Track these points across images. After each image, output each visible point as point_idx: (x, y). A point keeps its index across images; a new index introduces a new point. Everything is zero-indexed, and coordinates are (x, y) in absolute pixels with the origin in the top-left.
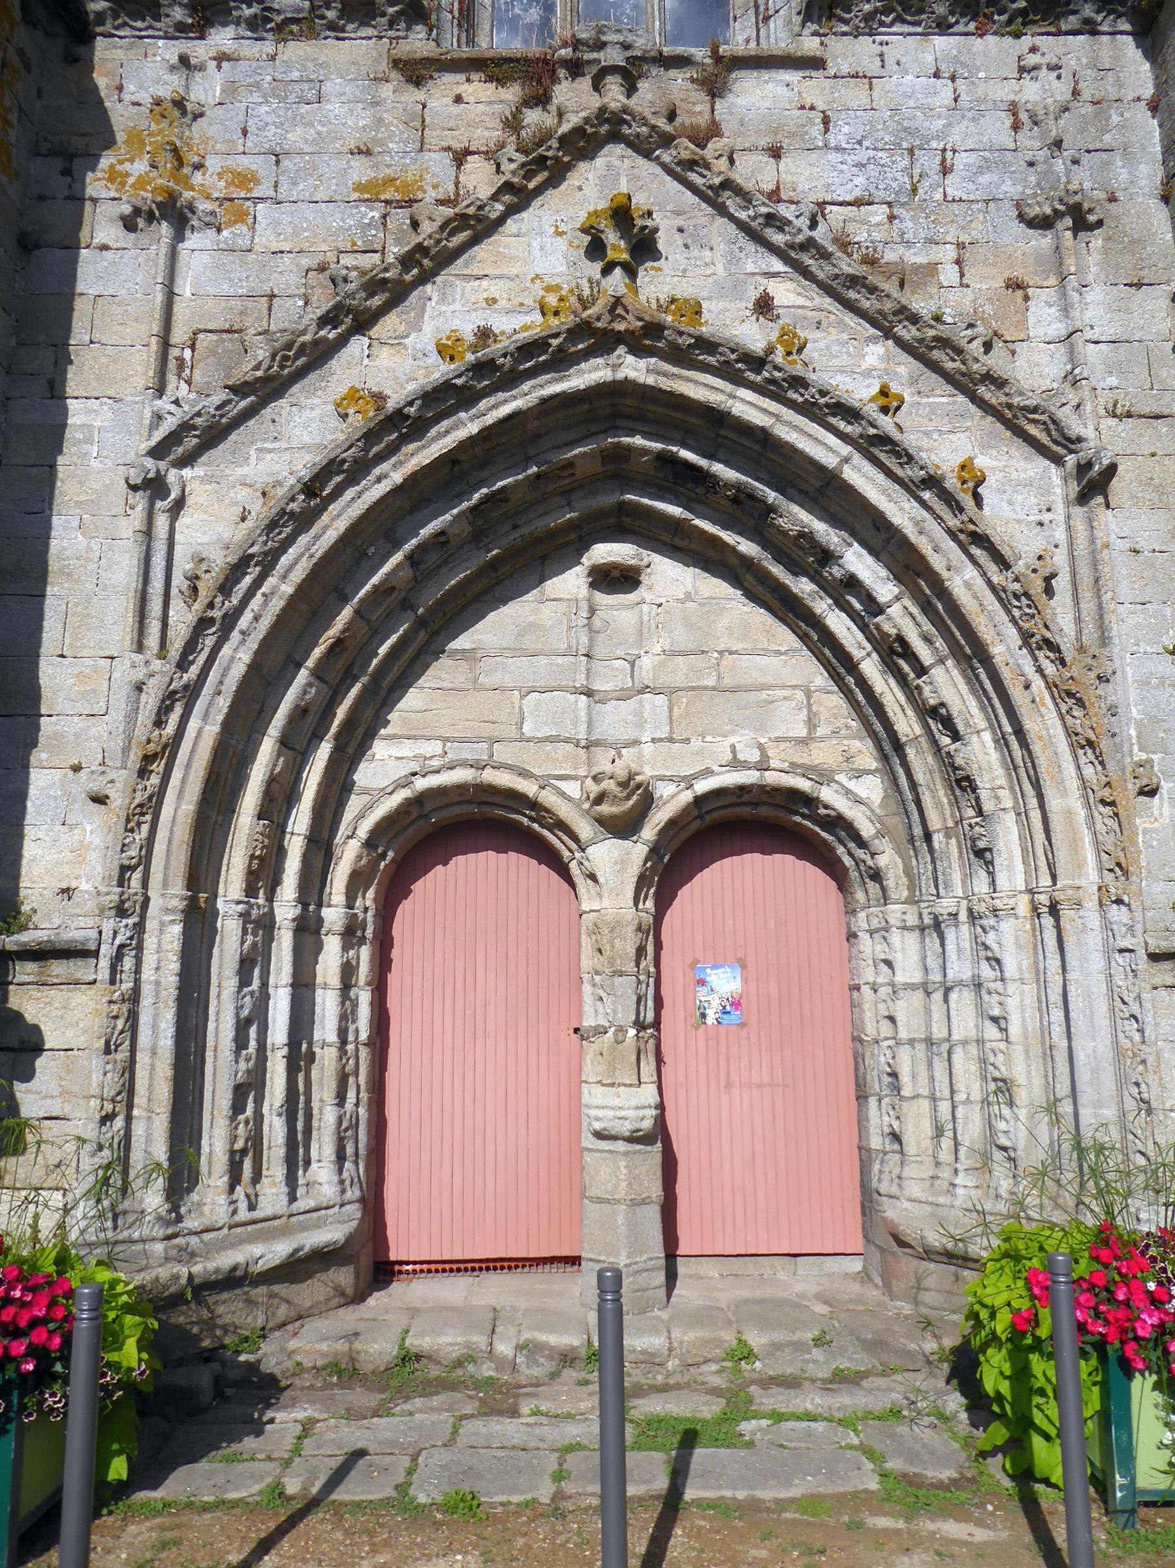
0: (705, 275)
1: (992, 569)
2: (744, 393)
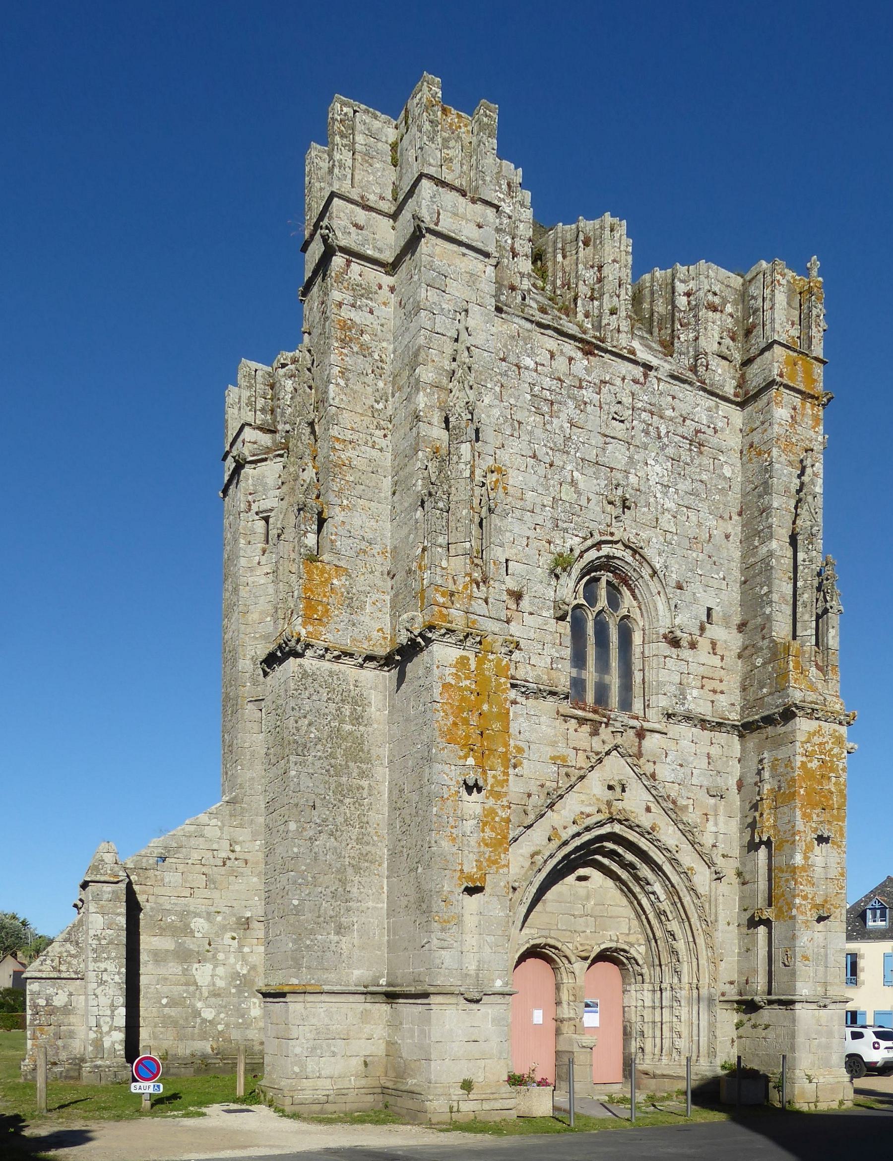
0: (635, 801)
1: (694, 898)
2: (643, 839)
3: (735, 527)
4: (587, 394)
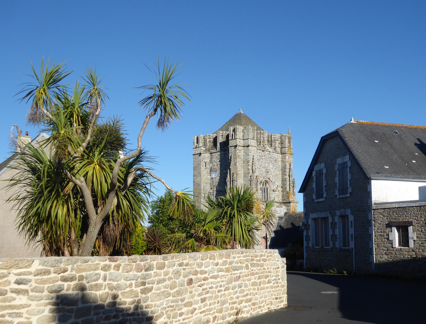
3: (280, 172)
4: (263, 157)
